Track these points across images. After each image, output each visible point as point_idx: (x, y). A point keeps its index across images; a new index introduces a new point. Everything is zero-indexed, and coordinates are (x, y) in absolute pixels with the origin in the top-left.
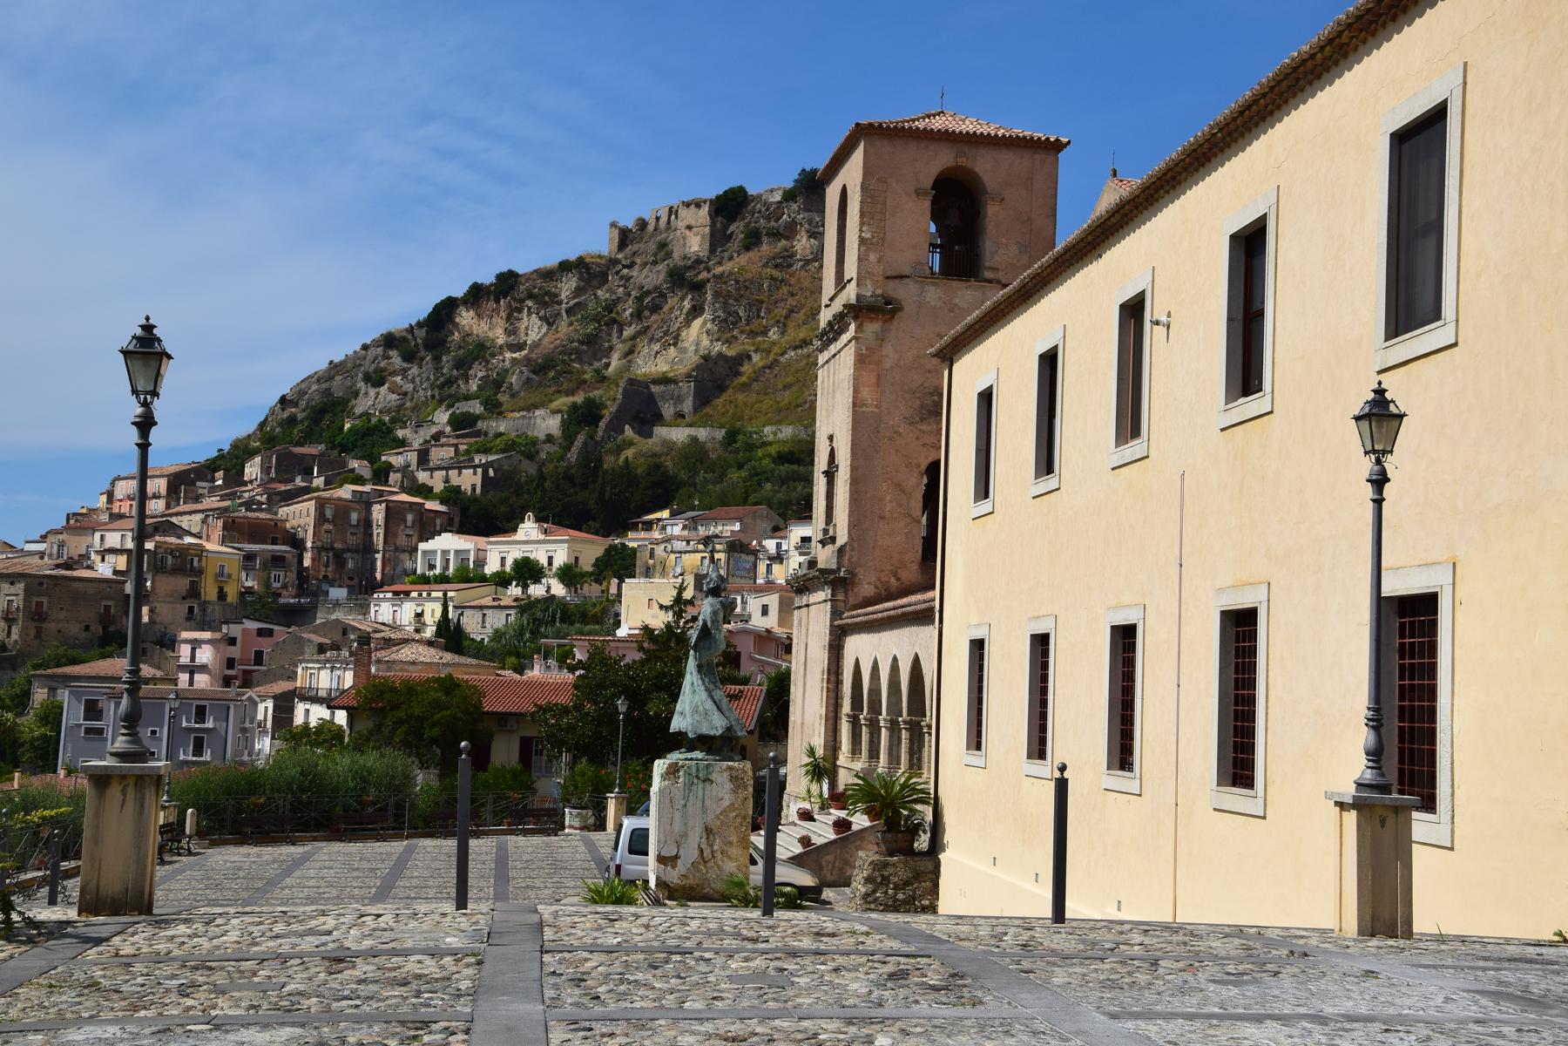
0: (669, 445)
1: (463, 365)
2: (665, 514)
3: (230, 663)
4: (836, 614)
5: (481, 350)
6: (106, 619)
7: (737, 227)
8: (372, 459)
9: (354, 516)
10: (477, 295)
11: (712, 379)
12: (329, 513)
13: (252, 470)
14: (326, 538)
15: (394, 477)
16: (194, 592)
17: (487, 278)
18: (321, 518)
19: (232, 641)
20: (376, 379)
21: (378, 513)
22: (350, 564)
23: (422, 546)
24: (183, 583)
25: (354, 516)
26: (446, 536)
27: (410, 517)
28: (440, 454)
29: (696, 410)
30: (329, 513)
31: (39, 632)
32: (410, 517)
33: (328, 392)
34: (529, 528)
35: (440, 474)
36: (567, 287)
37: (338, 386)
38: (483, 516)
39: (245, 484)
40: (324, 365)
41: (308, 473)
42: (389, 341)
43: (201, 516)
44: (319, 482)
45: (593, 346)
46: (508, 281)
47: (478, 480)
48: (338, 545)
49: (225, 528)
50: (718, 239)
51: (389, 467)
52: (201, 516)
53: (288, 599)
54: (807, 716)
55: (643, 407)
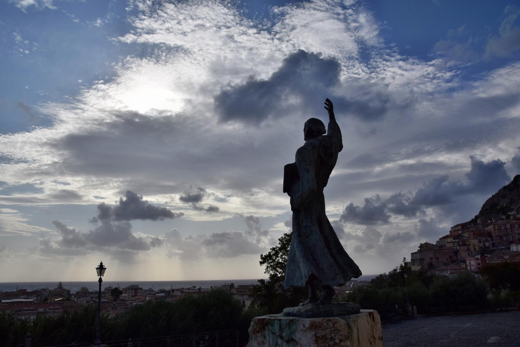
3: (479, 264)
6: (451, 257)
8: (505, 213)
9: (503, 228)
12: (497, 228)
13: (478, 221)
14: (497, 234)
15: (511, 217)
16: (468, 249)
18: (495, 229)
19: (478, 259)
21: (508, 226)
22: (504, 239)
24: (465, 248)
25: (503, 228)
27: (517, 226)
30: (497, 228)
31: (438, 262)
32: (517, 226)
39: (477, 224)
43: (468, 233)
44: (494, 221)
48: (500, 235)
49: (474, 234)
51: (510, 215)
52: (468, 233)
53: (491, 248)
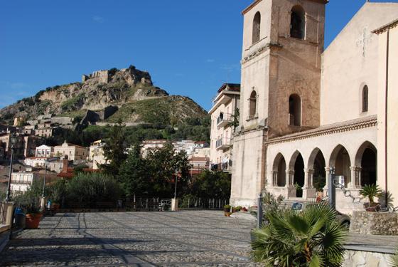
0: (99, 127)
1: (45, 106)
2: (100, 141)
4: (264, 140)
5: (49, 103)
7: (114, 77)
10: (49, 90)
11: (110, 112)
17: (52, 86)
20: (22, 109)
23: (37, 148)
26: (44, 146)
28: (41, 126)
29: (105, 118)
33: (9, 112)
34: (65, 145)
35: (41, 131)
36: (72, 89)
37: (12, 111)
38: (52, 142)
40: (8, 106)
41: (6, 130)
42: (25, 100)
45: (80, 102)
46: (57, 87)
47: (51, 133)
50: (110, 79)
54: (245, 174)
55: (93, 116)
